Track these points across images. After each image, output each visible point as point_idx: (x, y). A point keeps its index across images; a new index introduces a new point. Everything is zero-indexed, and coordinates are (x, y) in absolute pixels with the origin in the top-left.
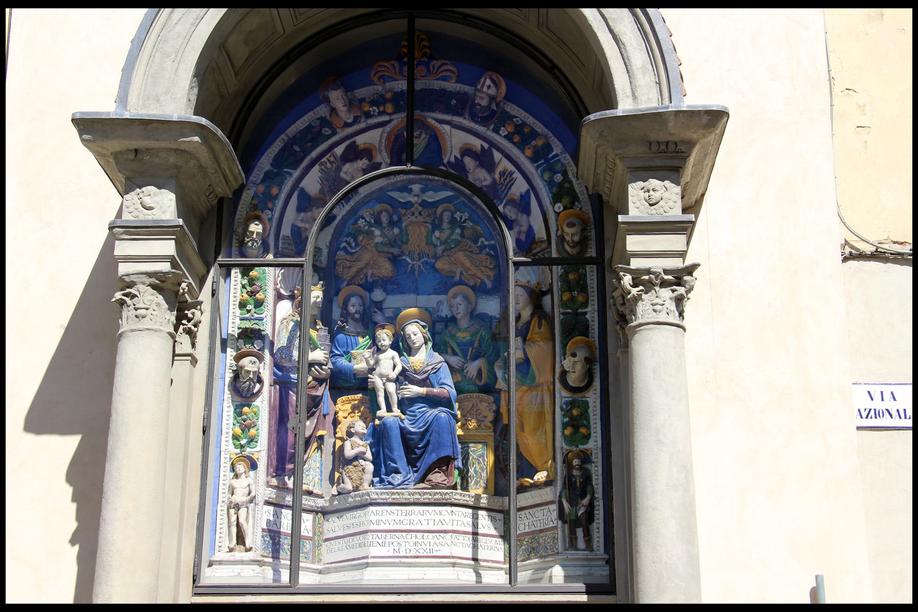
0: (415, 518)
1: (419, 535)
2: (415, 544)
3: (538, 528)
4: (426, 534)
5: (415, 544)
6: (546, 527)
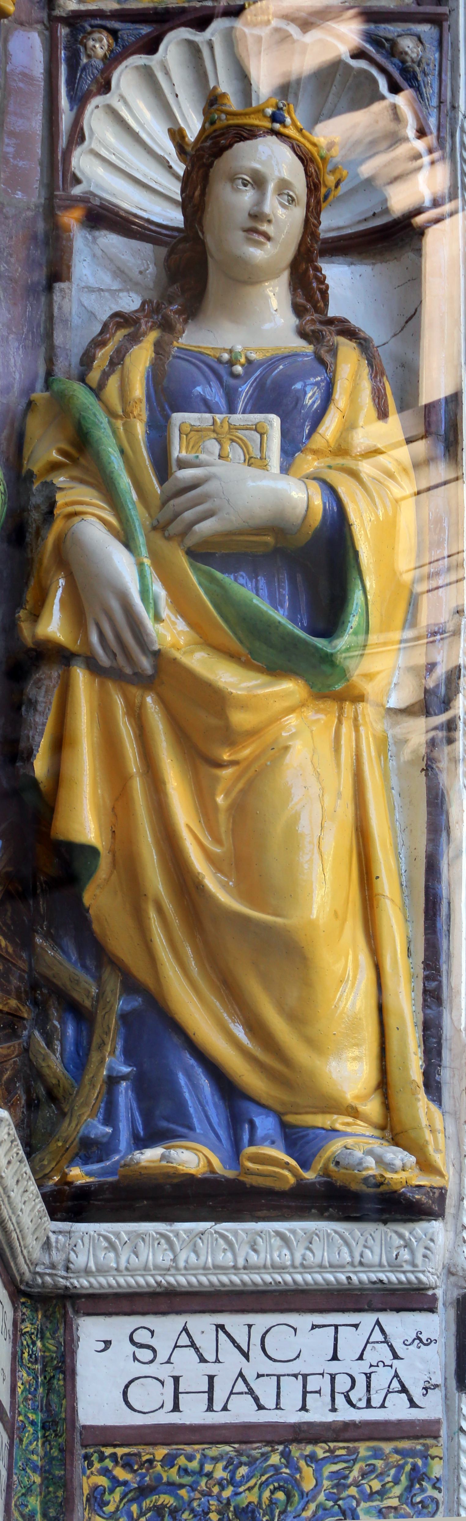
3: (291, 1415)
6: (345, 1414)
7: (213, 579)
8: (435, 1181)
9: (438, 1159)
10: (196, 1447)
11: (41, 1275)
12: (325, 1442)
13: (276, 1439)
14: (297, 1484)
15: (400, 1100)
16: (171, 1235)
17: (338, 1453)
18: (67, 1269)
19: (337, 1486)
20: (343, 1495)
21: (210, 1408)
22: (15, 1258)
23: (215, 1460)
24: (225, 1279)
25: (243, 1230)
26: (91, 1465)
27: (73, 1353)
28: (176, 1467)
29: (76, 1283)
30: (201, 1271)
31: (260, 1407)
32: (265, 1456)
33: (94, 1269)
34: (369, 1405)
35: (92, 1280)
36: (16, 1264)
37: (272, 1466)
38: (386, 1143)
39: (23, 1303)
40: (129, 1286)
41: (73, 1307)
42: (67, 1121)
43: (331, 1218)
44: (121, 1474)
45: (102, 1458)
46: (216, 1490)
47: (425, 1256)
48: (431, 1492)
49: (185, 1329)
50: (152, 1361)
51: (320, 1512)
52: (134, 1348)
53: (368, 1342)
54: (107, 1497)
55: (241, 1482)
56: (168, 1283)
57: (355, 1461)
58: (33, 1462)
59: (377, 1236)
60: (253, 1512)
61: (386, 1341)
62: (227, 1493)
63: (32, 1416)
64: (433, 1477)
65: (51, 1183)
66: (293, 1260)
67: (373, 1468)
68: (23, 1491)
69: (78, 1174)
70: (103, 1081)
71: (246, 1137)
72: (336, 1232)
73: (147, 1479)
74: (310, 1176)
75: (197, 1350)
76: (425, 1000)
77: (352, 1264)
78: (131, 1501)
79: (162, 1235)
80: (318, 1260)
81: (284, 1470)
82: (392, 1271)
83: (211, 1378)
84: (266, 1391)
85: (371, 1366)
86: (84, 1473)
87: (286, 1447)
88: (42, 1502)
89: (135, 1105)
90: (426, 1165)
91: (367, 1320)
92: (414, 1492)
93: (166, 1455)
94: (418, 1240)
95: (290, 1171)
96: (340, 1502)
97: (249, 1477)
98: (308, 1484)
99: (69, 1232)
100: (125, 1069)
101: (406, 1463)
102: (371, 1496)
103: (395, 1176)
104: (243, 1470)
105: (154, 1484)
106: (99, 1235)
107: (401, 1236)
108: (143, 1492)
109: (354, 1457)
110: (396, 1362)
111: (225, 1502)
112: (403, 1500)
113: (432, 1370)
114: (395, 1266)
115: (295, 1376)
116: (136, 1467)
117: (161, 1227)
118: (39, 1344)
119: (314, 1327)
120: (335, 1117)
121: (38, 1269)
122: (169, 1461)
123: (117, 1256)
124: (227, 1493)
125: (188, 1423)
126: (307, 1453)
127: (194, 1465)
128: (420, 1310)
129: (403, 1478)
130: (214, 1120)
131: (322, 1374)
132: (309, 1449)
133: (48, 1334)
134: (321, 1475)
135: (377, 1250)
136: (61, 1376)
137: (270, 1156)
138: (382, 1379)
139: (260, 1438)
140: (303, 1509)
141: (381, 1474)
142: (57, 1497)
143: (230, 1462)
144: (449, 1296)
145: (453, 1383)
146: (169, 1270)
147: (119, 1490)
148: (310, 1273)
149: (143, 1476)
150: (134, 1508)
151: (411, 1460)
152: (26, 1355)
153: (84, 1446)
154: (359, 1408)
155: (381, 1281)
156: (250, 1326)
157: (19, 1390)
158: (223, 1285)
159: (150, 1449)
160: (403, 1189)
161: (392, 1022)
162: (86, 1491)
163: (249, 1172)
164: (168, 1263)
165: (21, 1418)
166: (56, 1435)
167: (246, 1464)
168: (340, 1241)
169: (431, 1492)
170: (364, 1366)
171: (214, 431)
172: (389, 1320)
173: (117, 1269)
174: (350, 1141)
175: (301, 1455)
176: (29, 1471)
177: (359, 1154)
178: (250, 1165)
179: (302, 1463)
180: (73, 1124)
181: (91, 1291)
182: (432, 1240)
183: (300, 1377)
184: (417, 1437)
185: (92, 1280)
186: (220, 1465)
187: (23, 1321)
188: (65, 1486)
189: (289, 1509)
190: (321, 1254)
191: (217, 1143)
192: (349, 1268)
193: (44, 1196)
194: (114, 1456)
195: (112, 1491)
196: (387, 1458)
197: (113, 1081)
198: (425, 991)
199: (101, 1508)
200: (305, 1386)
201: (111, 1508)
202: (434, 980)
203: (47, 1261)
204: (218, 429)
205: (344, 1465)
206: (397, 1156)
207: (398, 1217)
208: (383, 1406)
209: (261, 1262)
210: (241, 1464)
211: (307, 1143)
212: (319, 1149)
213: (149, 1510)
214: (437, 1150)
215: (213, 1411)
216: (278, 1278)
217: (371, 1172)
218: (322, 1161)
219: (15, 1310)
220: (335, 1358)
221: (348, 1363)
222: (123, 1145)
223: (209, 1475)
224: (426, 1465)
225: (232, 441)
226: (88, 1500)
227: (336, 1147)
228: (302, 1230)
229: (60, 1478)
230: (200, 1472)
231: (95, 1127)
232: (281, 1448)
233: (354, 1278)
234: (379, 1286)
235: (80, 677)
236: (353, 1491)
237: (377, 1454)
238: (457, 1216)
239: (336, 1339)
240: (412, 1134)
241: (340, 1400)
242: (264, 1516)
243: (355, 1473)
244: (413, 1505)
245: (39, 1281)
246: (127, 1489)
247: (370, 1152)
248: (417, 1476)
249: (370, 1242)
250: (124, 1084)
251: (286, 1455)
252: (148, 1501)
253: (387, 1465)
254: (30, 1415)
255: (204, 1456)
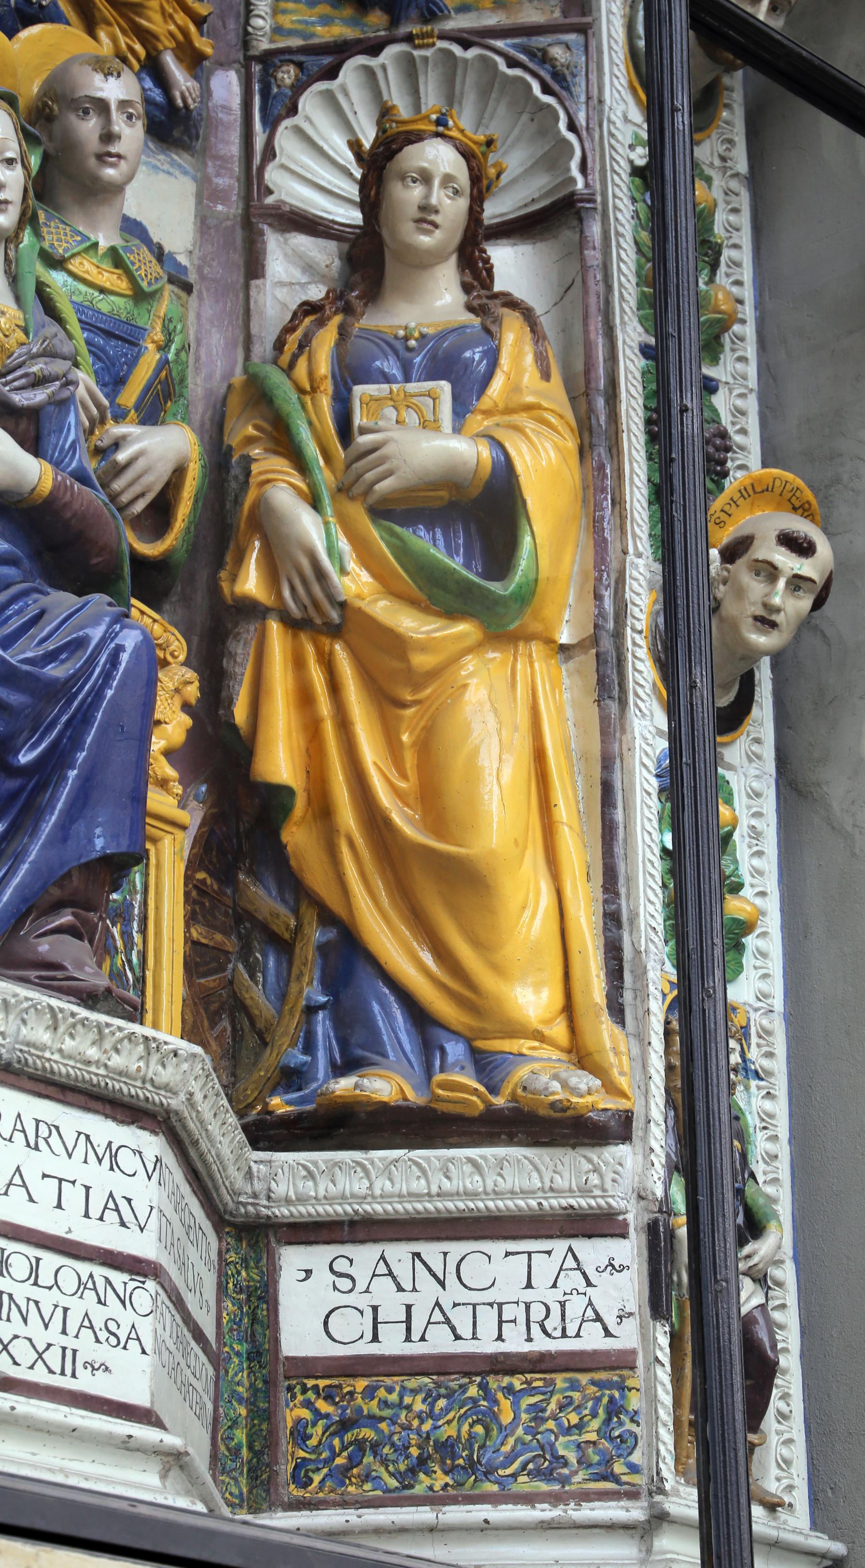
3: (488, 1346)
4: (50, 1261)
6: (541, 1344)
7: (393, 534)
8: (622, 1104)
9: (623, 1082)
10: (396, 1378)
11: (245, 1205)
12: (522, 1373)
13: (473, 1370)
14: (495, 1417)
15: (585, 1023)
16: (366, 1162)
17: (535, 1384)
18: (269, 1198)
19: (534, 1419)
20: (542, 1429)
21: (408, 1339)
22: (217, 1189)
23: (415, 1392)
24: (419, 1206)
25: (435, 1157)
26: (294, 1397)
27: (276, 1282)
28: (377, 1400)
29: (277, 1213)
30: (396, 1199)
31: (458, 1337)
32: (463, 1388)
33: (294, 1198)
34: (564, 1335)
35: (293, 1209)
36: (219, 1195)
37: (471, 1398)
38: (573, 1067)
39: (228, 1233)
40: (328, 1214)
41: (275, 1237)
42: (268, 1050)
43: (520, 1144)
44: (323, 1406)
45: (304, 1390)
46: (415, 1423)
47: (614, 1181)
48: (629, 1426)
49: (383, 1258)
50: (351, 1291)
51: (519, 1447)
52: (334, 1277)
53: (561, 1269)
54: (309, 1430)
55: (440, 1414)
56: (365, 1211)
57: (552, 1393)
58: (239, 1394)
59: (566, 1160)
60: (452, 1446)
61: (579, 1268)
62: (427, 1426)
63: (237, 1347)
64: (630, 1409)
65: (254, 1112)
66: (485, 1187)
67: (570, 1401)
68: (229, 1424)
69: (280, 1104)
70: (302, 1011)
71: (438, 1063)
72: (526, 1158)
73: (348, 1411)
74: (499, 1101)
75: (394, 1278)
76: (605, 923)
77: (542, 1189)
78: (333, 1434)
79: (358, 1164)
80: (509, 1186)
81: (482, 1403)
82: (582, 1197)
83: (409, 1308)
84: (462, 1320)
85: (565, 1294)
86: (287, 1405)
87: (483, 1378)
88: (247, 1435)
89: (332, 1034)
90: (611, 1088)
91: (560, 1246)
92: (612, 1425)
93: (367, 1387)
94: (606, 1164)
95: (479, 1097)
96: (539, 1437)
97: (447, 1410)
98: (507, 1417)
99: (270, 1162)
100: (323, 999)
101: (603, 1395)
102: (568, 1431)
103: (581, 1100)
104: (442, 1403)
105: (354, 1416)
106: (298, 1164)
107: (590, 1161)
108: (345, 1425)
109: (551, 1388)
110: (589, 1289)
111: (424, 1435)
112: (602, 1434)
113: (626, 1298)
114: (585, 1191)
115: (491, 1305)
116: (337, 1399)
117: (357, 1155)
118: (244, 1273)
119: (508, 1254)
120: (522, 1041)
121: (241, 1199)
122: (370, 1393)
123: (316, 1184)
124: (427, 1426)
125: (387, 1353)
126: (504, 1384)
127: (394, 1397)
128: (612, 1236)
129: (601, 1411)
130: (408, 1047)
131: (517, 1303)
132: (506, 1380)
133: (252, 1264)
134: (519, 1408)
135: (566, 1175)
136: (265, 1306)
137: (459, 1083)
138: (577, 1305)
139: (458, 1370)
140: (502, 1444)
141: (579, 1407)
142: (262, 1430)
143: (429, 1394)
144: (640, 1220)
145: (647, 1311)
146: (365, 1198)
147: (321, 1423)
148: (502, 1199)
149: (344, 1409)
150: (336, 1442)
151: (608, 1392)
152: (231, 1285)
153: (287, 1378)
154: (554, 1338)
155: (572, 1207)
156: (445, 1254)
157: (225, 1321)
158: (418, 1212)
159: (351, 1381)
160: (590, 1114)
161: (574, 946)
162: (290, 1424)
163: (438, 1099)
164: (364, 1191)
165: (227, 1349)
166: (260, 1366)
167: (444, 1397)
168: (531, 1167)
169: (629, 1426)
170: (558, 1294)
171: (391, 399)
172: (581, 1246)
173: (316, 1198)
174: (536, 1066)
175: (499, 1386)
176: (234, 1403)
177: (544, 1078)
178: (440, 1092)
179: (500, 1395)
180: (274, 1054)
181: (292, 1220)
182: (620, 1164)
183: (495, 1306)
184: (613, 1368)
185: (293, 1209)
186: (419, 1398)
187: (228, 1250)
188: (269, 1419)
189: (488, 1443)
190: (512, 1180)
191: (410, 1070)
192: (540, 1194)
193: (245, 1128)
194: (316, 1388)
195: (314, 1424)
196: (584, 1390)
197: (311, 1010)
198: (605, 915)
199: (304, 1442)
200: (500, 1315)
201: (313, 1442)
202: (613, 903)
203: (249, 1190)
204: (395, 398)
205: (541, 1397)
206: (583, 1080)
207: (586, 1141)
208: (578, 1335)
209: (455, 1189)
210: (439, 1396)
211: (496, 1067)
212: (507, 1074)
213: (351, 1444)
214: (622, 1073)
215: (411, 1341)
216: (471, 1205)
217: (557, 1097)
218: (511, 1086)
219: (220, 1239)
220: (529, 1286)
221: (542, 1292)
222: (321, 1074)
223: (409, 1408)
224: (623, 1397)
225: (408, 407)
226: (291, 1433)
227: (522, 1072)
228: (493, 1156)
229: (265, 1411)
230: (400, 1405)
231: (295, 1056)
232: (478, 1379)
233: (545, 1203)
234: (570, 1211)
235: (274, 627)
236: (551, 1424)
237: (574, 1386)
238: (645, 1139)
239: (529, 1266)
240: (597, 1057)
241: (536, 1329)
242: (463, 1450)
243: (553, 1406)
244: (611, 1439)
245: (243, 1210)
246: (329, 1423)
247: (556, 1077)
248: (615, 1410)
249: (560, 1167)
250: (321, 1015)
251: (483, 1387)
252: (349, 1434)
253: (584, 1397)
254: (235, 1346)
255: (403, 1388)
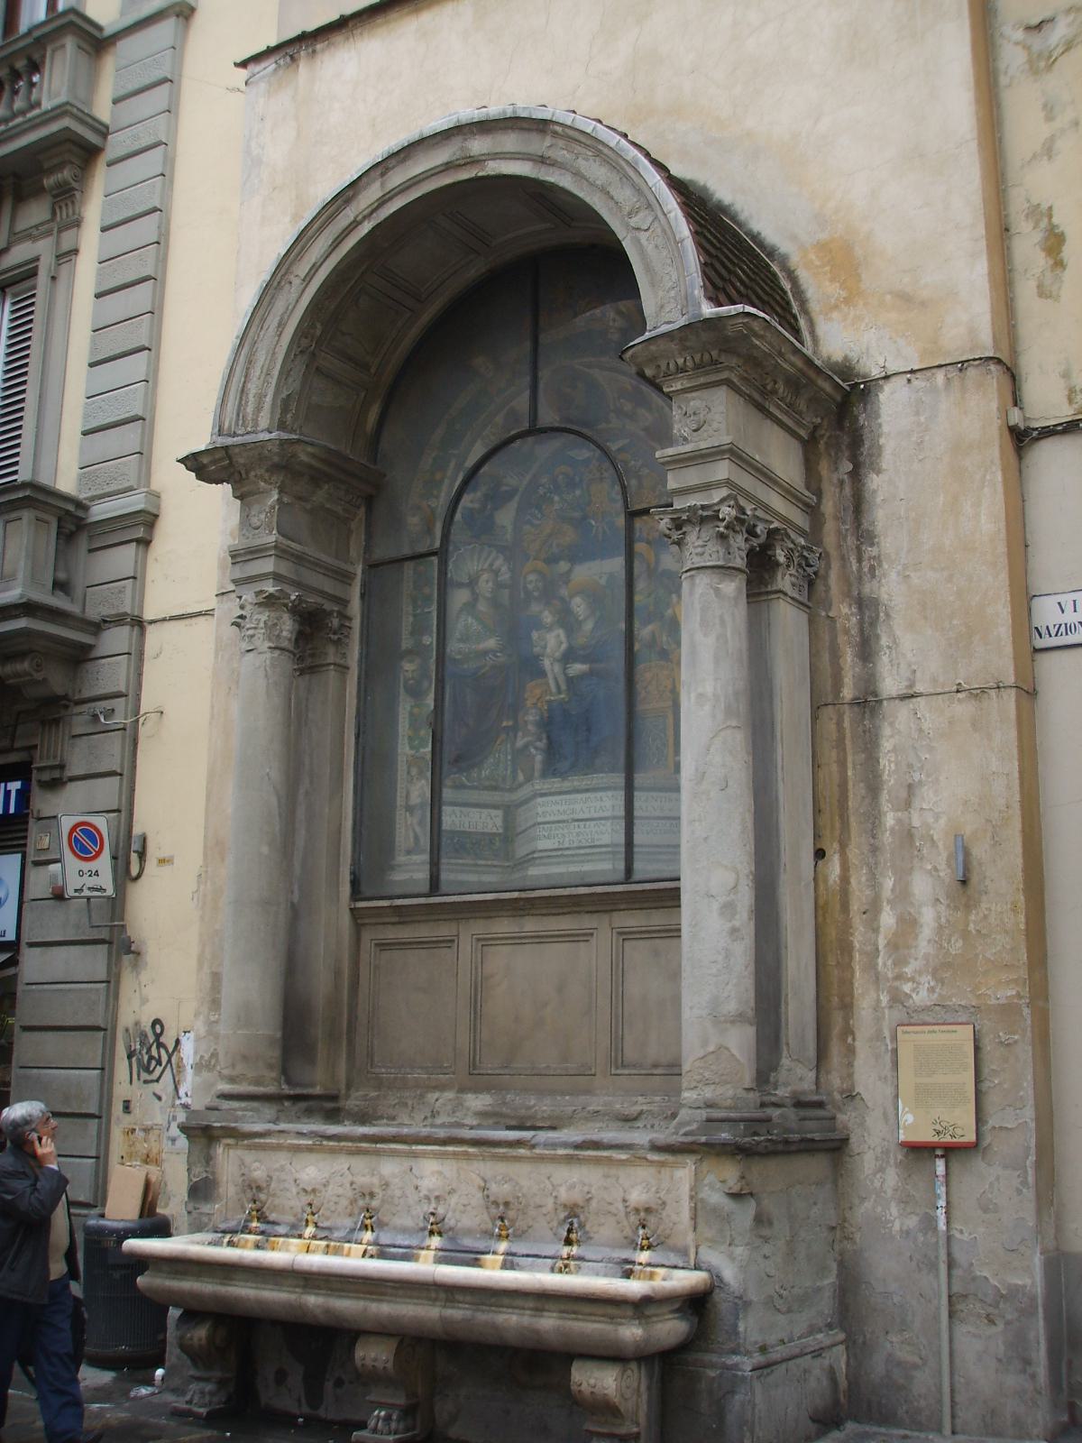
0: (577, 807)
1: (582, 824)
2: (578, 834)
4: (588, 823)
5: (578, 834)
